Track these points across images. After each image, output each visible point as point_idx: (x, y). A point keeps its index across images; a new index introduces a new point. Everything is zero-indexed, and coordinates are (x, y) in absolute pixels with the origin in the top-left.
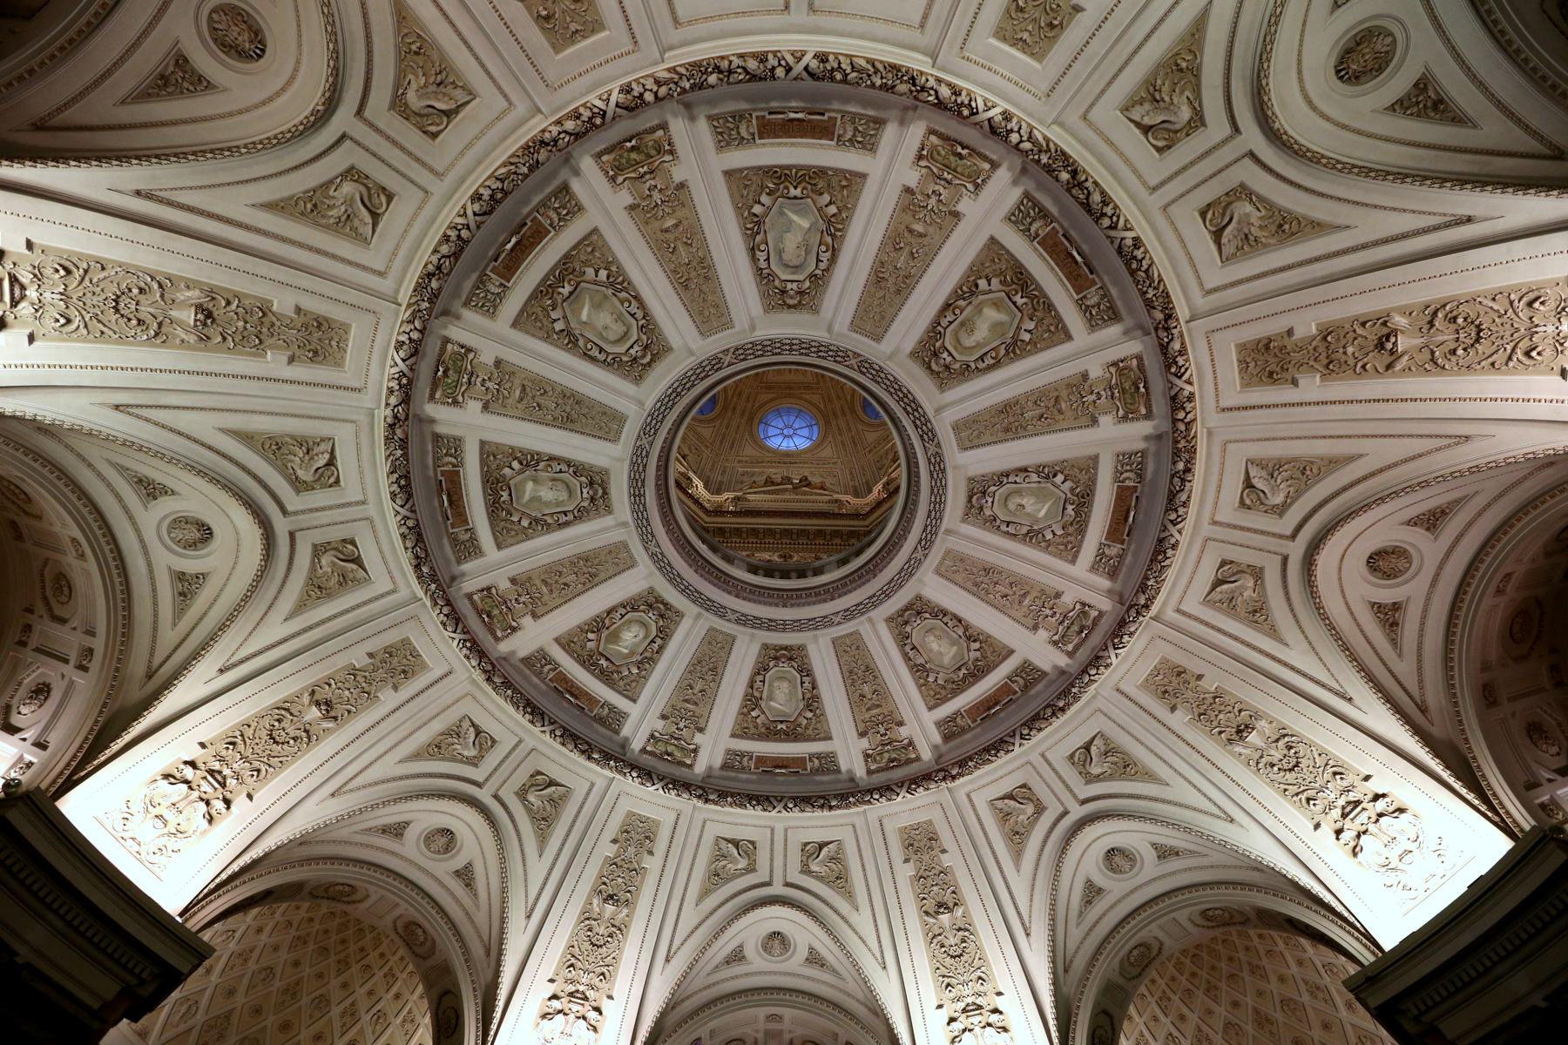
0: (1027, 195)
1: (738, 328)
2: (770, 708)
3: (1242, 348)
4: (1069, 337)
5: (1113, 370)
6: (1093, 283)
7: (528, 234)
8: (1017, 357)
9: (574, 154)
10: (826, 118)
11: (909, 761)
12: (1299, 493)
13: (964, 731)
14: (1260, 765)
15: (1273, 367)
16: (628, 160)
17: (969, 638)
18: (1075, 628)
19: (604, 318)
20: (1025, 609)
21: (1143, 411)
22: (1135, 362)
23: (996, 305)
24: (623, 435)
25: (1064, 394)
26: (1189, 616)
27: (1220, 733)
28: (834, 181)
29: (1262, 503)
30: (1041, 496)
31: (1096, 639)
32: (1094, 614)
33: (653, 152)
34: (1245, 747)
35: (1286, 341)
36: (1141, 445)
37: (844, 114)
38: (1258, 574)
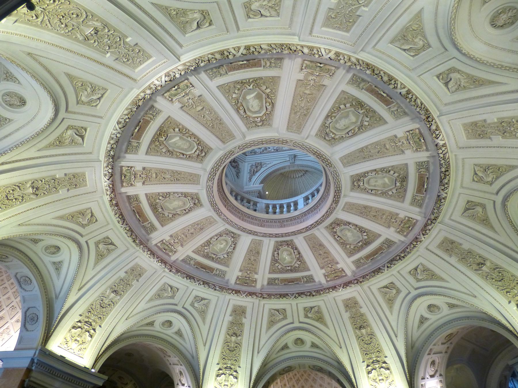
0: (314, 281)
1: (340, 211)
2: (175, 136)
3: (246, 307)
4: (270, 273)
5: (254, 280)
7: (422, 189)
8: (272, 260)
9: (424, 219)
10: (370, 260)
11: (122, 182)
12: (197, 310)
13: (130, 203)
14: (102, 298)
15: (237, 312)
16: (408, 224)
17: (175, 215)
18: (166, 248)
19: (380, 182)
20: (180, 234)
21: (237, 282)
22: (254, 285)
23: (291, 262)
24: (340, 163)
25: (254, 267)
27: (115, 286)
28: (354, 251)
29: (195, 301)
30: (222, 250)
31: (160, 253)
32: (170, 254)
33: (403, 229)
34: (109, 293)
37: (367, 264)
38: (172, 297)
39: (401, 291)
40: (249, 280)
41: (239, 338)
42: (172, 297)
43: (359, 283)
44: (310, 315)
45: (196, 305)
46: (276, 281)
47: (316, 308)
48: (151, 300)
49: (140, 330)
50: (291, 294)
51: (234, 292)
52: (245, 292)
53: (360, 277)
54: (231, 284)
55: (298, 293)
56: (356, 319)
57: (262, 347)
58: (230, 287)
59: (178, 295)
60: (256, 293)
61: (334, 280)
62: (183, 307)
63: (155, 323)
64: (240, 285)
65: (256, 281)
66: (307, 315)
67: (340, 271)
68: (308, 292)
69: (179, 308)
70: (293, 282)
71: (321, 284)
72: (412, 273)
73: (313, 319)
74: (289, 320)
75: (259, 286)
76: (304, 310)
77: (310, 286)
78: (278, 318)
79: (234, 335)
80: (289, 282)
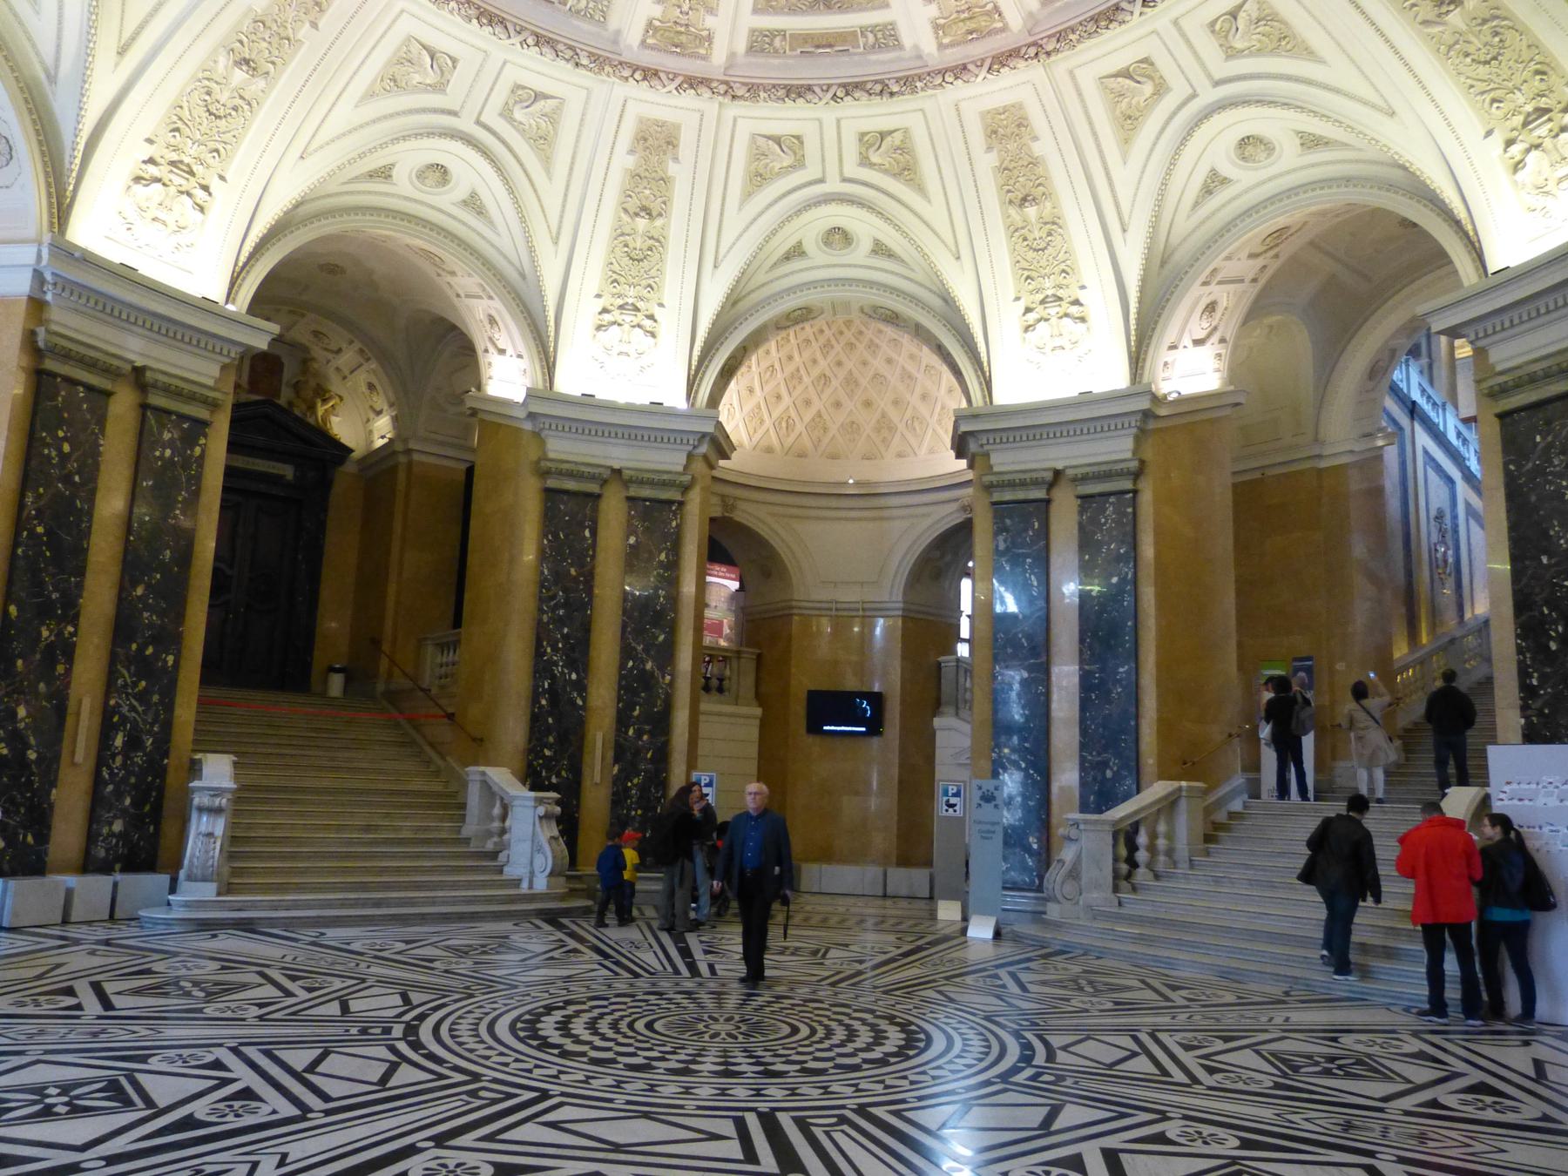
0: (899, 46)
3: (678, 127)
4: (756, 11)
5: (705, 33)
6: (792, 49)
12: (522, 132)
15: (650, 141)
21: (650, 41)
22: (702, 51)
26: (394, 21)
27: (241, 42)
29: (516, 102)
34: (226, 67)
35: (669, 155)
36: (614, 23)
38: (439, 87)
39: (1168, 90)
40: (687, 33)
41: (659, 222)
42: (439, 87)
43: (1042, 57)
44: (875, 158)
45: (519, 114)
46: (777, 42)
47: (898, 136)
48: (370, 95)
49: (352, 193)
50: (820, 86)
51: (638, 76)
52: (676, 75)
53: (1049, 37)
54: (630, 47)
55: (844, 86)
56: (1016, 172)
57: (728, 252)
58: (626, 57)
59: (458, 82)
60: (712, 80)
61: (966, 42)
62: (478, 122)
63: (394, 173)
64: (660, 50)
65: (709, 38)
66: (867, 158)
67: (988, 14)
68: (876, 82)
69: (466, 124)
70: (830, 46)
71: (919, 57)
72: (1217, 27)
73: (886, 172)
74: (812, 172)
75: (719, 56)
76: (860, 140)
77: (883, 63)
78: (777, 166)
79: (643, 214)
80: (818, 47)
